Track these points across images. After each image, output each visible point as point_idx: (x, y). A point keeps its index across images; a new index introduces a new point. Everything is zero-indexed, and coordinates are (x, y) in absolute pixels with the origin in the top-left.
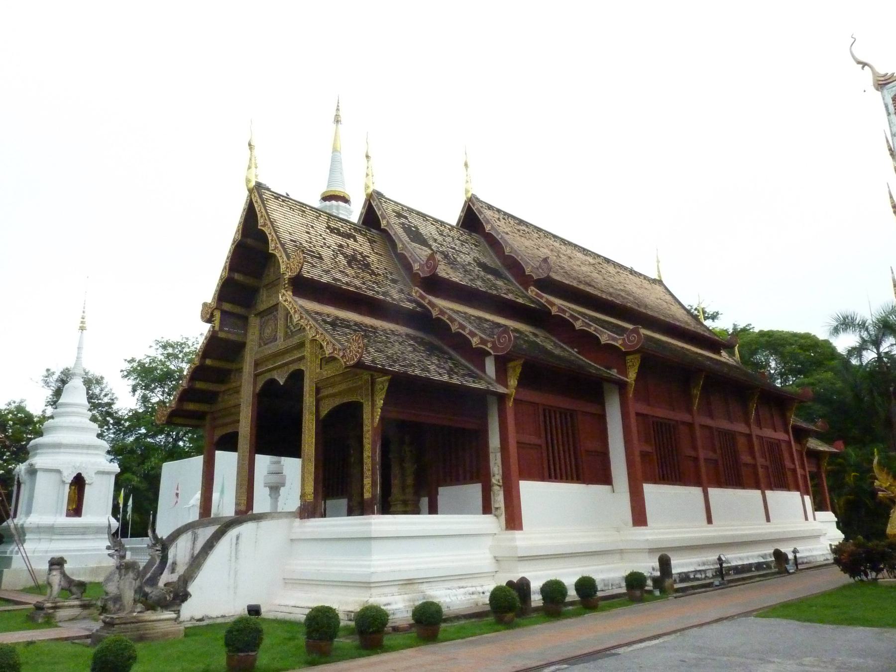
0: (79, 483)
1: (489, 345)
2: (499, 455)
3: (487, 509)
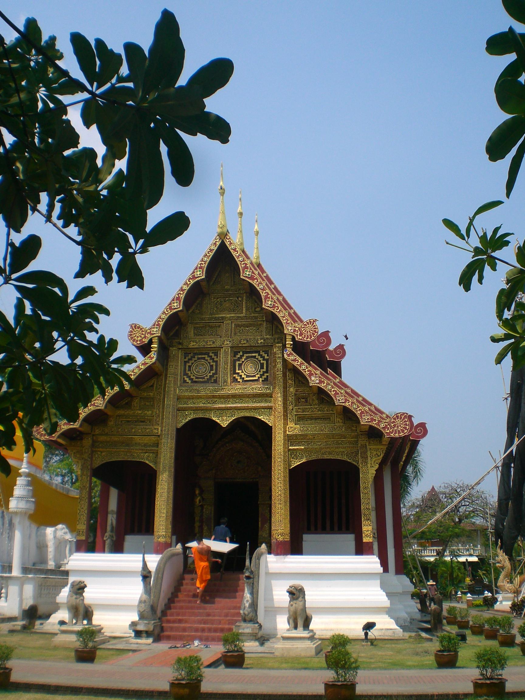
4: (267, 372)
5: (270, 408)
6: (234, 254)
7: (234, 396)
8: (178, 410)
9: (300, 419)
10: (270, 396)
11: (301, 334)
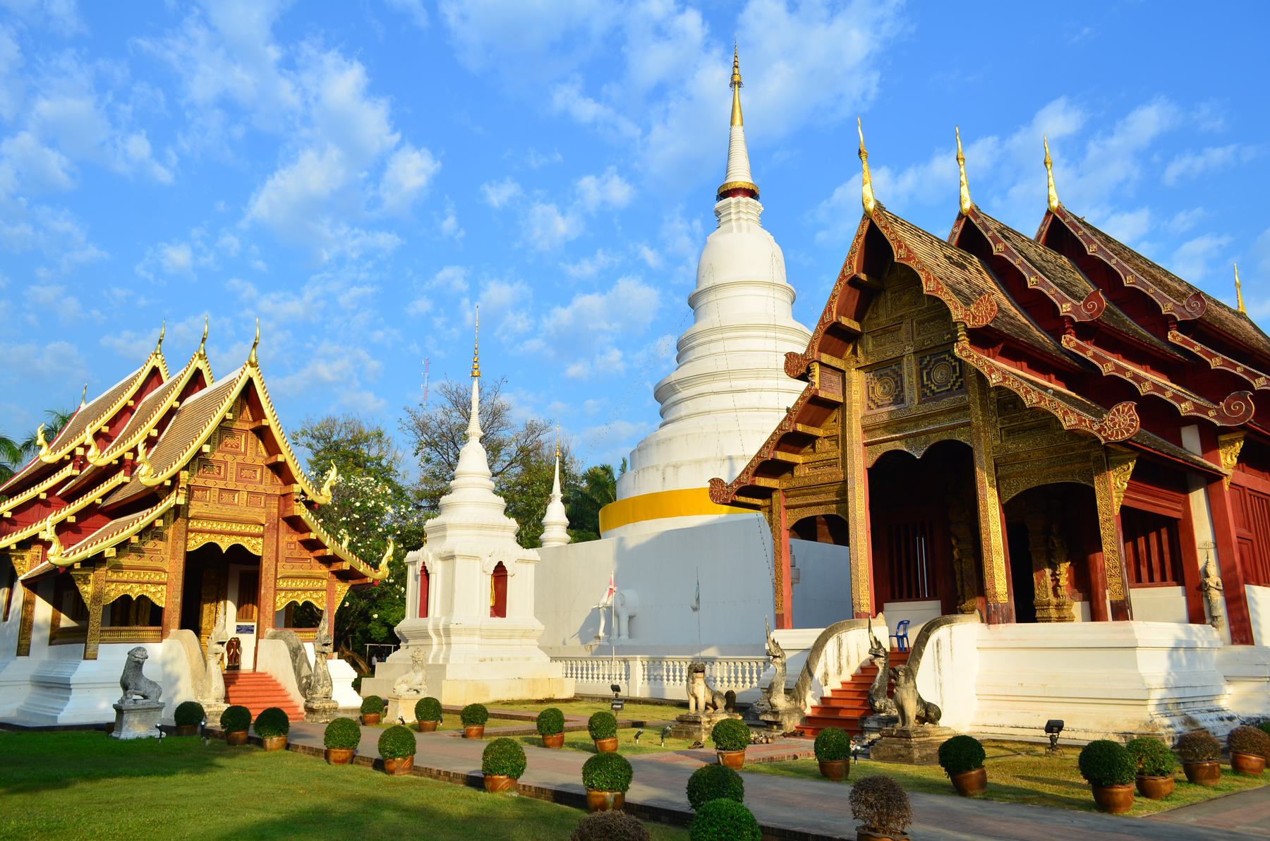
0: (500, 573)
1: (1211, 413)
2: (1212, 553)
3: (1197, 614)
4: (961, 376)
5: (969, 424)
6: (884, 232)
7: (925, 417)
8: (866, 445)
9: (1010, 433)
10: (967, 408)
11: (974, 318)
